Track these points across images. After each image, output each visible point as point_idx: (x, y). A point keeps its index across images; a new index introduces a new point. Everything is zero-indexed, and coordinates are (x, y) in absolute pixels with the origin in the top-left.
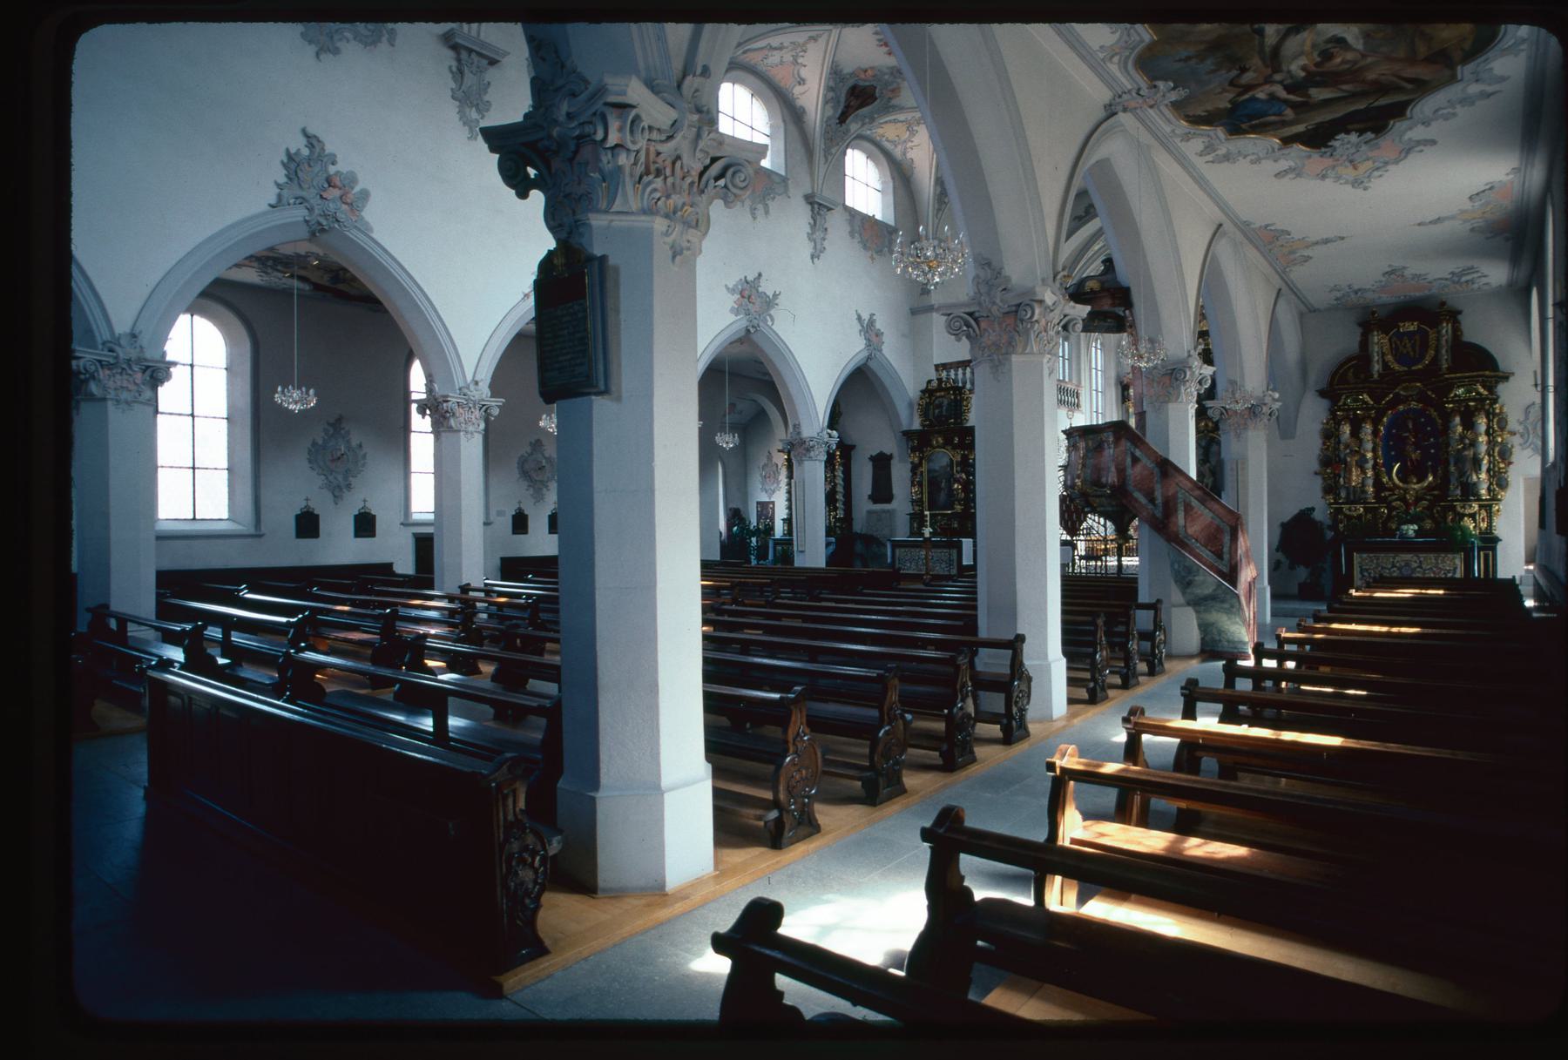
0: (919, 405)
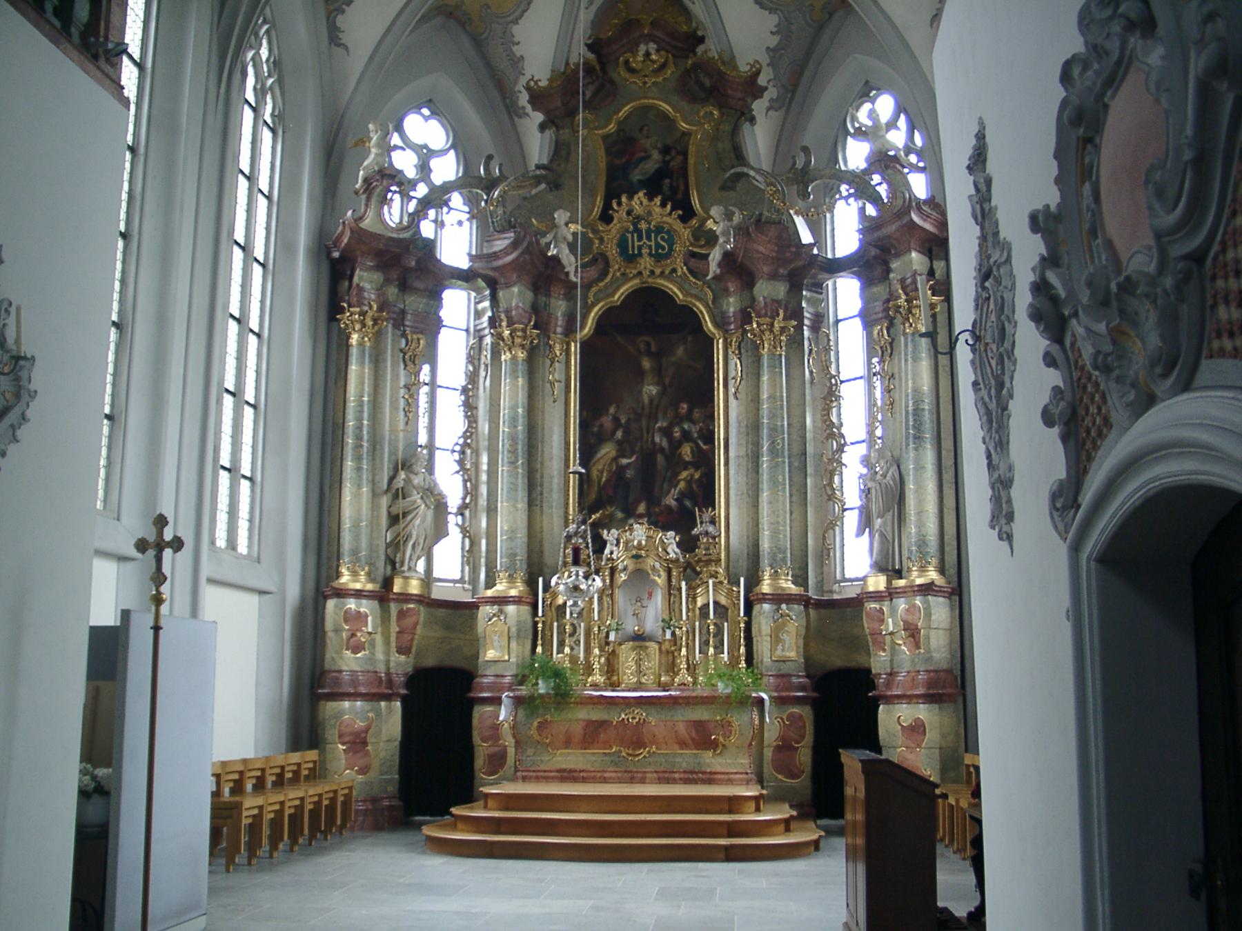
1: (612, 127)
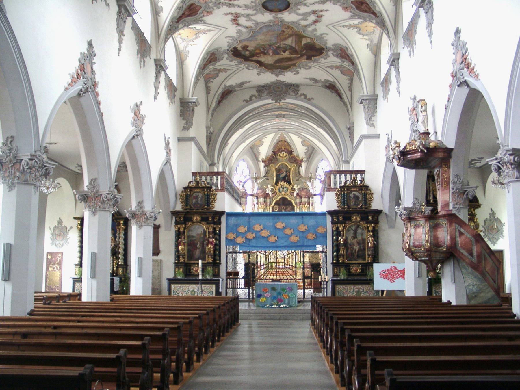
0: (181, 195)
1: (277, 167)
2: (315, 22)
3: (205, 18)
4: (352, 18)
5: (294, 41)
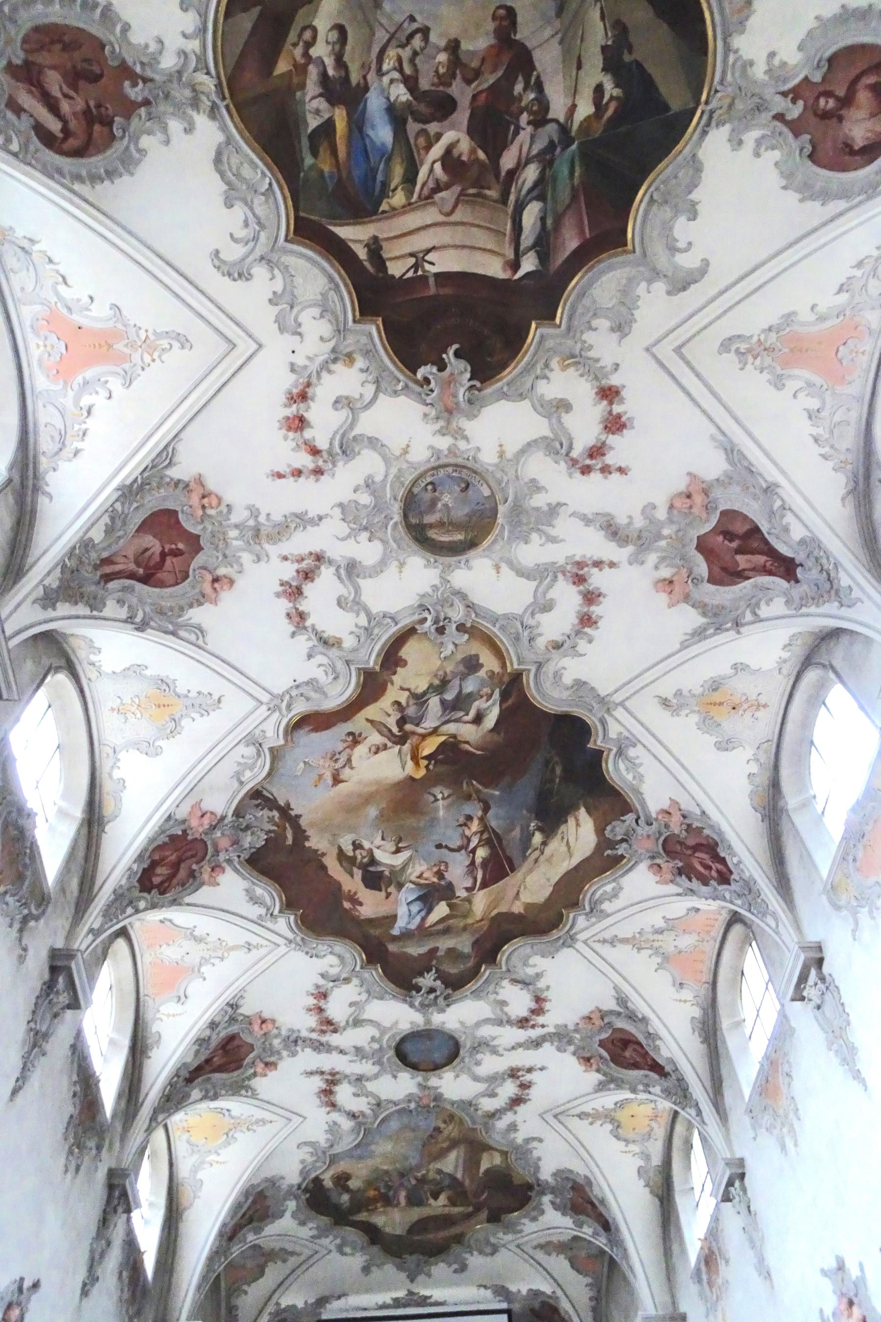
2: (517, 1101)
3: (256, 1083)
4: (601, 1087)
5: (461, 1161)
